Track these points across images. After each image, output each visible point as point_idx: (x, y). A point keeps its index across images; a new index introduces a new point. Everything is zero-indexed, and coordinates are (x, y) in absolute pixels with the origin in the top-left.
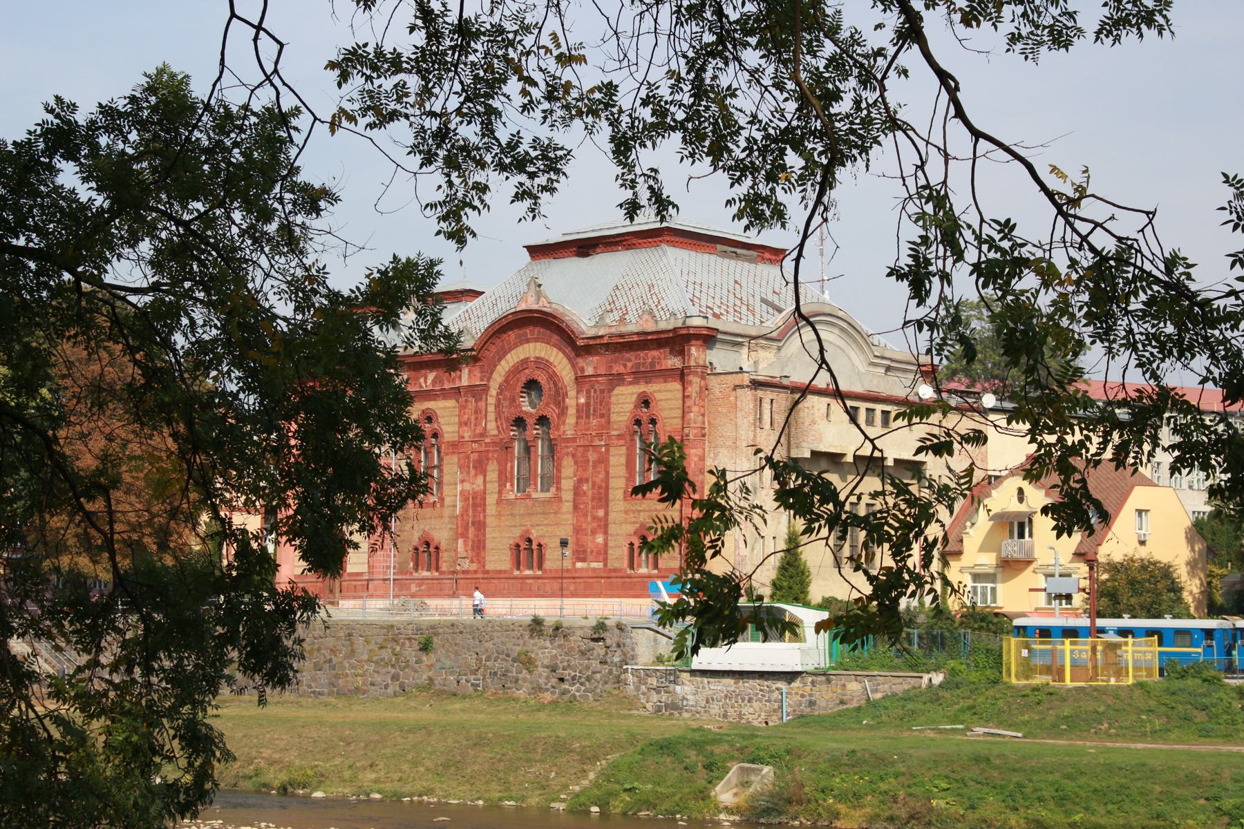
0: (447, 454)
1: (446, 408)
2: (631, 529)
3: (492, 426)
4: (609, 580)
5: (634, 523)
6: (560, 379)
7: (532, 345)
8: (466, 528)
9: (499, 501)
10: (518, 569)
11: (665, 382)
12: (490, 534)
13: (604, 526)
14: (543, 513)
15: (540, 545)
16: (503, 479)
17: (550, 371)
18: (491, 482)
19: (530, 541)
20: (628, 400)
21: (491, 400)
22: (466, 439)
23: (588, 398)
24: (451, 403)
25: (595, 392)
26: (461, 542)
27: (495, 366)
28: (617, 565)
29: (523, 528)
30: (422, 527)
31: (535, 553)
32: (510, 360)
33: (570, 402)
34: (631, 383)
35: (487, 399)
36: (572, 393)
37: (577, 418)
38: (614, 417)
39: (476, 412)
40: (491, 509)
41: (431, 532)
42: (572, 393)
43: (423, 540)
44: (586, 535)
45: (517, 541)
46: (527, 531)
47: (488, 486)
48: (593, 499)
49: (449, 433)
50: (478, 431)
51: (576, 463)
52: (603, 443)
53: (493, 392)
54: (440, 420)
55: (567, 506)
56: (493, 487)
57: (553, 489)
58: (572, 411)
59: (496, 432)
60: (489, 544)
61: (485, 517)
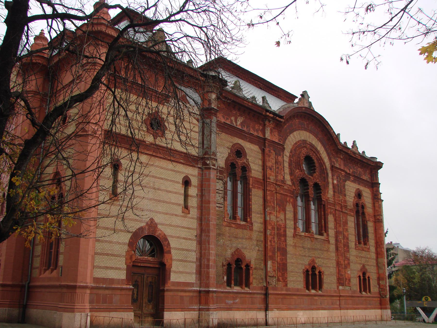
0: (254, 187)
1: (252, 149)
2: (359, 267)
3: (288, 177)
4: (353, 298)
5: (360, 264)
6: (324, 163)
7: (308, 134)
8: (274, 253)
9: (295, 235)
10: (308, 288)
11: (365, 187)
12: (290, 260)
13: (349, 264)
14: (320, 250)
15: (320, 272)
16: (295, 220)
17: (318, 155)
18: (289, 219)
19: (314, 268)
20: (352, 190)
21: (286, 159)
22: (272, 181)
23: (338, 181)
24: (255, 148)
25: (340, 179)
26: (269, 263)
27: (288, 136)
28: (355, 289)
29: (310, 258)
30: (234, 245)
31: (318, 276)
32: (296, 137)
33: (330, 180)
34: (352, 181)
35: (283, 157)
36: (330, 175)
37: (334, 192)
38: (348, 198)
39: (276, 163)
40: (290, 241)
41: (242, 250)
42: (330, 175)
43: (236, 258)
44: (343, 268)
45: (308, 267)
46: (313, 261)
47: (288, 222)
48: (344, 245)
49: (255, 170)
50: (280, 178)
51: (335, 220)
52: (346, 212)
53: (287, 153)
54: (248, 158)
55: (332, 247)
56: (290, 224)
57: (325, 234)
58: (331, 186)
59: (289, 183)
60: (290, 268)
61: (286, 245)
